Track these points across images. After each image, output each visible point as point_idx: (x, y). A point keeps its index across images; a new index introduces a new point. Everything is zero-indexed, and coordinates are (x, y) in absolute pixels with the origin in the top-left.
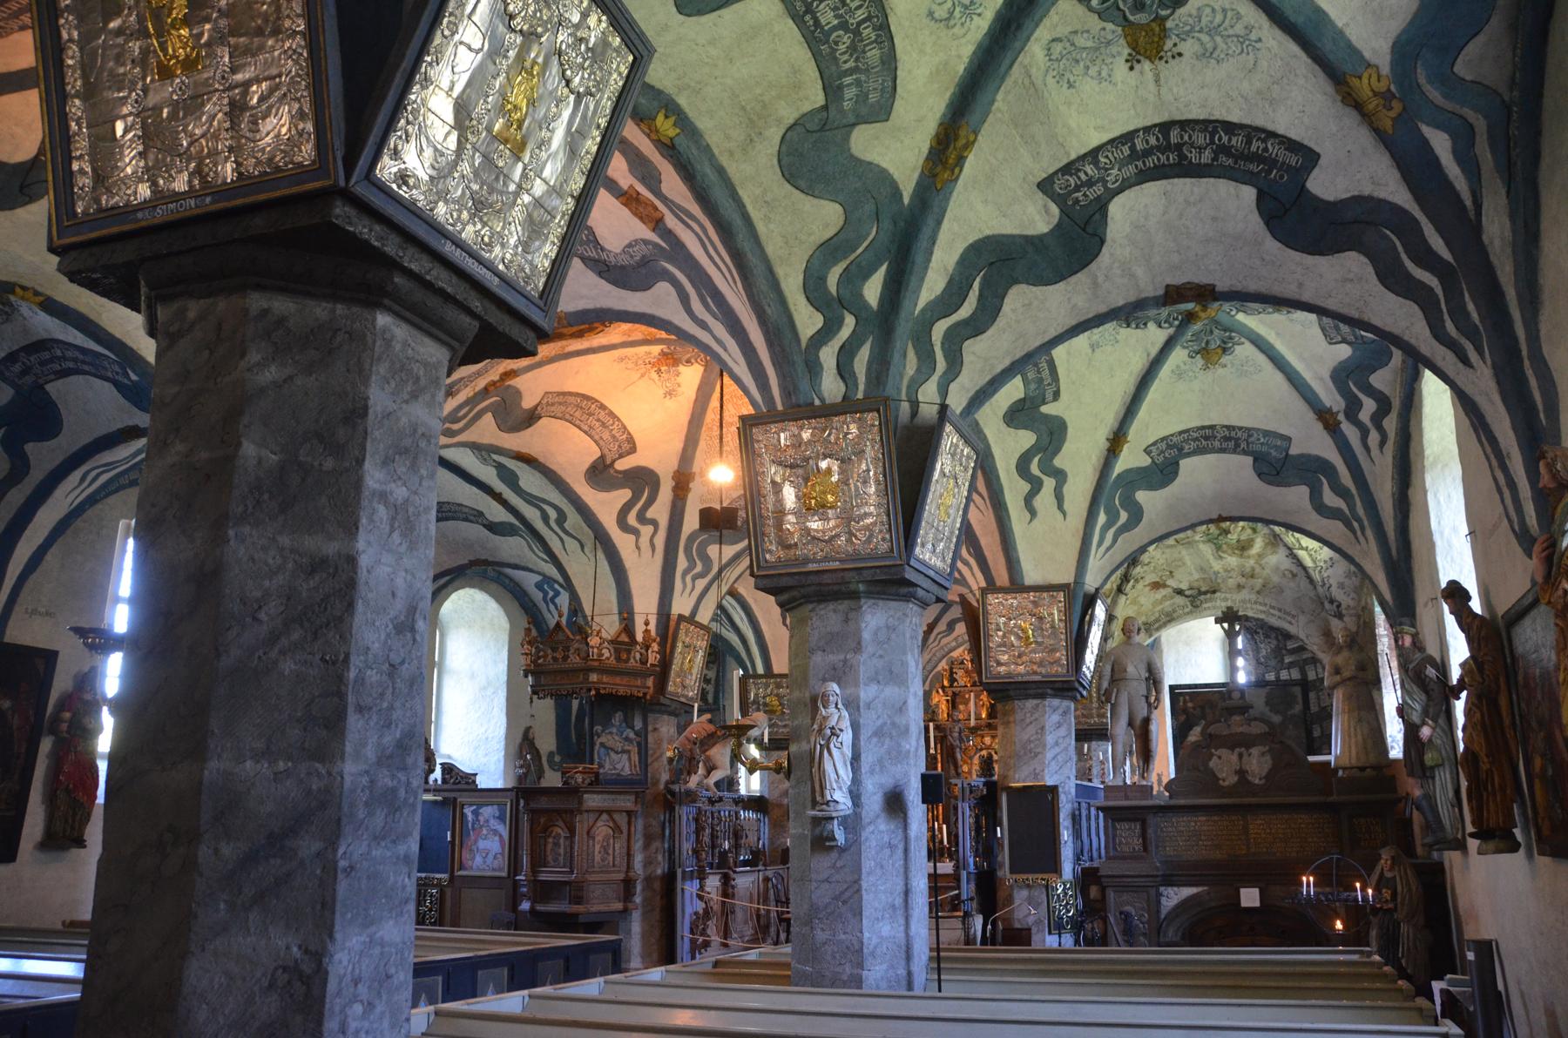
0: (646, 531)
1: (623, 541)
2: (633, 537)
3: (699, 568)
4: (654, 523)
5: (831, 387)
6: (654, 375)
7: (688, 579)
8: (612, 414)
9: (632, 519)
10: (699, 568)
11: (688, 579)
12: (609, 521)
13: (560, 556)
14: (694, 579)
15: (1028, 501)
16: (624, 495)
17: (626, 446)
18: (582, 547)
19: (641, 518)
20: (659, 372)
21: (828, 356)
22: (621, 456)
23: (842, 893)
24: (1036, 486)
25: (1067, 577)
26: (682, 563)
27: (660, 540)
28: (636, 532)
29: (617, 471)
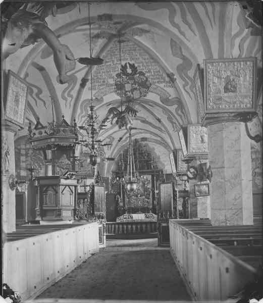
0: (69, 99)
1: (62, 102)
2: (65, 101)
3: (84, 114)
4: (71, 96)
5: (236, 52)
7: (80, 117)
9: (66, 95)
10: (84, 114)
11: (80, 117)
12: (59, 94)
13: (34, 107)
14: (82, 118)
17: (73, 67)
18: (45, 103)
21: (237, 41)
23: (236, 213)
26: (79, 111)
27: (72, 104)
29: (68, 76)
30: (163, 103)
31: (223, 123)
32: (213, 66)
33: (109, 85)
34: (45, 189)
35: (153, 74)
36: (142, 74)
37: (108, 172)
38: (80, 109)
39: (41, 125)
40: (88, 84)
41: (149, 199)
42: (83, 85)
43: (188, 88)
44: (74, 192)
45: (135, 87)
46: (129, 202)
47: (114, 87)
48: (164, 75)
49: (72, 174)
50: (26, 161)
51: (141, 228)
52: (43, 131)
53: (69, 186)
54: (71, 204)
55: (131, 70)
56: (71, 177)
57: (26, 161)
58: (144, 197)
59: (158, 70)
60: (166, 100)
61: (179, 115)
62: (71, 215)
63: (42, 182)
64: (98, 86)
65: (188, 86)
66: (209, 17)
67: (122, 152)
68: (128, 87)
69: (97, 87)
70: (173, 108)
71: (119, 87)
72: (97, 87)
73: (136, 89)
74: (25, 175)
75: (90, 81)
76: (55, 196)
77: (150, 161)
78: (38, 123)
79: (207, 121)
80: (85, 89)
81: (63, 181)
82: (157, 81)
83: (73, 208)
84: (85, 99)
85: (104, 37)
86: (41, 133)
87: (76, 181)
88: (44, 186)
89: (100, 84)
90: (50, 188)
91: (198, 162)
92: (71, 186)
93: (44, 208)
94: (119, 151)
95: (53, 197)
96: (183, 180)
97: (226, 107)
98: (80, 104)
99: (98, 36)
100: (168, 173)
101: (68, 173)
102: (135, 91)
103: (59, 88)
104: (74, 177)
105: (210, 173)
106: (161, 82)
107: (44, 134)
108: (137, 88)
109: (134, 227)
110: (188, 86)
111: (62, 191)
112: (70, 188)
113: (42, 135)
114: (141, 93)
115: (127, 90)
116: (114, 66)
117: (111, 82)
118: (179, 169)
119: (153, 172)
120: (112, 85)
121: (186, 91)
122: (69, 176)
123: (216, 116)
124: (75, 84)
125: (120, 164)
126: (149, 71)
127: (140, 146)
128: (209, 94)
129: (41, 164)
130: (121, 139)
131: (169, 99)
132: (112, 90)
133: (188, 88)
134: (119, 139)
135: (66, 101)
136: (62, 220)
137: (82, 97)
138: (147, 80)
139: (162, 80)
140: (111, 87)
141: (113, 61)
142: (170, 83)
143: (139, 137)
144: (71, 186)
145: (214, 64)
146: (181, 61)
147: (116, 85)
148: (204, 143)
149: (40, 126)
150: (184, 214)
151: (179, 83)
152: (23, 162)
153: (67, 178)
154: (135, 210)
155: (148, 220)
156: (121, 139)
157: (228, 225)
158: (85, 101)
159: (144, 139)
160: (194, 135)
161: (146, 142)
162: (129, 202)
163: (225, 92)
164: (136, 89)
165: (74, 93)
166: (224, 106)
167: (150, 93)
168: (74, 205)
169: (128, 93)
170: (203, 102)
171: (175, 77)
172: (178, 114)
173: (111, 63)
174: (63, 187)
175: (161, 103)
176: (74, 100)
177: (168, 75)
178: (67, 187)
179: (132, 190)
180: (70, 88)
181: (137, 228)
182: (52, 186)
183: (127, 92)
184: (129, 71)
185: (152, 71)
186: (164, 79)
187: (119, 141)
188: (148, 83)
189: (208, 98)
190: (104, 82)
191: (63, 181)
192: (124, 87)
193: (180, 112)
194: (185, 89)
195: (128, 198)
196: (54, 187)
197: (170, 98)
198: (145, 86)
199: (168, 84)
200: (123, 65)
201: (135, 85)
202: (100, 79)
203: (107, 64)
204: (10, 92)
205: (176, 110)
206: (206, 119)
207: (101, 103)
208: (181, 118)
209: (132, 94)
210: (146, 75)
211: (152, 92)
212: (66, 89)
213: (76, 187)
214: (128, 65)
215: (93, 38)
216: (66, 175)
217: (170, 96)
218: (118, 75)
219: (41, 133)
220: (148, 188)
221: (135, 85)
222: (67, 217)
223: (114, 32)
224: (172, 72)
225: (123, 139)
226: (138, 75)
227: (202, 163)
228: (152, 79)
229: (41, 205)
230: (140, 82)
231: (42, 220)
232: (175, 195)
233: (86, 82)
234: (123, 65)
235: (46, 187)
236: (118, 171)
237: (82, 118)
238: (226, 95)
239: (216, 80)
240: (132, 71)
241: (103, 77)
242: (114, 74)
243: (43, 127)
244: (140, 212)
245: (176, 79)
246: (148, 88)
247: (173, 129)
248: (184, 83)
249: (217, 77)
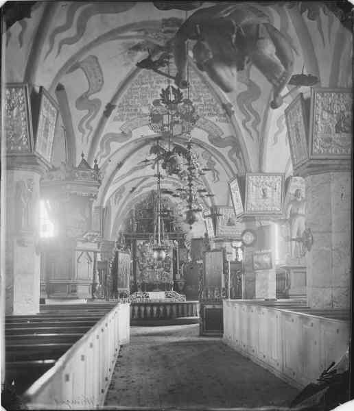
0: (87, 131)
3: (104, 153)
4: (91, 129)
6: (127, 53)
8: (101, 71)
10: (104, 153)
12: (75, 123)
14: (101, 158)
15: (276, 135)
16: (85, 112)
19: (88, 124)
20: (129, 53)
22: (94, 93)
24: (280, 131)
25: (282, 171)
26: (98, 148)
27: (90, 139)
28: (84, 133)
30: (212, 143)
31: (331, 173)
32: (322, 96)
33: (142, 115)
35: (203, 103)
36: (188, 102)
37: (114, 234)
40: (115, 112)
41: (169, 272)
42: (107, 113)
43: (249, 124)
44: (93, 260)
45: (176, 120)
46: (142, 275)
47: (148, 118)
48: (218, 106)
49: (93, 236)
51: (165, 310)
53: (87, 251)
54: (90, 276)
55: (174, 96)
56: (91, 239)
58: (162, 269)
59: (210, 98)
60: (216, 140)
61: (234, 161)
62: (88, 291)
64: (128, 115)
65: (250, 122)
66: (321, 33)
67: (133, 208)
68: (166, 120)
69: (126, 116)
70: (225, 151)
71: (155, 118)
72: (126, 116)
73: (177, 122)
75: (117, 109)
77: (172, 221)
79: (310, 169)
80: (110, 118)
82: (207, 112)
83: (92, 282)
84: (108, 132)
85: (145, 50)
87: (96, 245)
89: (130, 112)
91: (257, 224)
92: (91, 251)
94: (130, 205)
96: (235, 248)
97: (336, 152)
98: (101, 139)
99: (137, 48)
100: (195, 237)
101: (88, 234)
102: (176, 125)
103: (77, 114)
104: (95, 239)
105: (310, 238)
106: (214, 115)
108: (178, 121)
109: (155, 309)
110: (250, 122)
111: (79, 258)
112: (88, 255)
114: (183, 128)
115: (165, 122)
116: (152, 90)
117: (146, 111)
118: (219, 232)
119: (176, 235)
120: (146, 115)
121: (247, 130)
122: (88, 238)
123: (324, 163)
124: (96, 113)
125: (131, 223)
126: (199, 100)
128: (316, 134)
130: (134, 189)
131: (220, 138)
132: (145, 123)
133: (249, 124)
134: (131, 189)
135: (84, 133)
136: (77, 298)
137: (104, 131)
138: (194, 109)
139: (215, 113)
140: (145, 118)
141: (151, 83)
142: (224, 116)
144: (91, 251)
145: (325, 95)
146: (245, 88)
147: (151, 116)
148: (267, 198)
150: (237, 295)
151: (238, 117)
153: (86, 241)
154: (152, 287)
155: (168, 300)
156: (134, 189)
157: (335, 308)
158: (108, 134)
160: (254, 187)
162: (142, 275)
163: (337, 132)
164: (177, 122)
165: (94, 123)
166: (333, 151)
167: (195, 129)
168: (92, 278)
169: (166, 128)
170: (308, 143)
171: (233, 109)
172: (231, 158)
173: (149, 86)
175: (209, 143)
176: (92, 134)
177: (224, 106)
178: (85, 254)
179: (160, 259)
180: (90, 117)
181: (158, 310)
183: (164, 125)
184: (172, 97)
185: (202, 99)
186: (217, 110)
187: (131, 192)
188: (195, 116)
189: (314, 139)
190: (136, 110)
192: (162, 118)
193: (234, 156)
194: (244, 126)
195: (141, 270)
197: (222, 137)
198: (191, 118)
199: (222, 118)
200: (165, 90)
201: (177, 116)
202: (131, 106)
203: (144, 86)
204: (41, 117)
205: (230, 153)
206: (309, 167)
207: (128, 139)
208: (236, 165)
209: (172, 129)
210: (193, 105)
211: (199, 127)
212: (86, 117)
213: (95, 252)
214: (171, 89)
215: (130, 49)
216: (85, 236)
217: (223, 134)
218: (156, 103)
220: (169, 257)
221: (177, 116)
222: (84, 294)
223: (162, 44)
224: (229, 101)
225: (137, 190)
226: (183, 103)
227: (263, 225)
228: (201, 110)
230: (184, 113)
231: (49, 298)
232: (225, 268)
233: (112, 110)
234: (165, 90)
236: (127, 233)
237: (101, 158)
238: (337, 135)
239: (326, 115)
240: (175, 97)
241: (136, 103)
242: (151, 101)
244: (158, 290)
245: (233, 112)
246: (195, 121)
247: (212, 179)
248: (244, 118)
249: (328, 112)
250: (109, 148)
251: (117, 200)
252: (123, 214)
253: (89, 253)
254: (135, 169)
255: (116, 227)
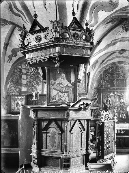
34: (45, 124)
37: (91, 88)
38: (90, 15)
39: (40, 26)
44: (86, 128)
49: (87, 105)
50: (27, 78)
52: (42, 35)
53: (79, 121)
57: (27, 78)
63: (41, 115)
67: (102, 73)
74: (26, 91)
76: (60, 137)
78: (35, 23)
81: (73, 115)
86: (39, 39)
88: (44, 120)
90: (53, 124)
93: (44, 154)
95: (57, 138)
107: (43, 41)
113: (42, 42)
122: (82, 107)
127: (117, 67)
129: (38, 81)
134: (101, 62)
143: (116, 60)
149: (38, 28)
152: (24, 79)
156: (103, 61)
159: (120, 62)
161: (121, 65)
174: (72, 122)
182: (56, 121)
187: (101, 63)
191: (73, 115)
196: (60, 123)
219: (39, 39)
229: (39, 147)
235: (47, 122)
243: (43, 30)
250: (97, 17)
251: (93, 69)
252: (97, 76)
253: (82, 122)
254: (108, 46)
255: (92, 84)
